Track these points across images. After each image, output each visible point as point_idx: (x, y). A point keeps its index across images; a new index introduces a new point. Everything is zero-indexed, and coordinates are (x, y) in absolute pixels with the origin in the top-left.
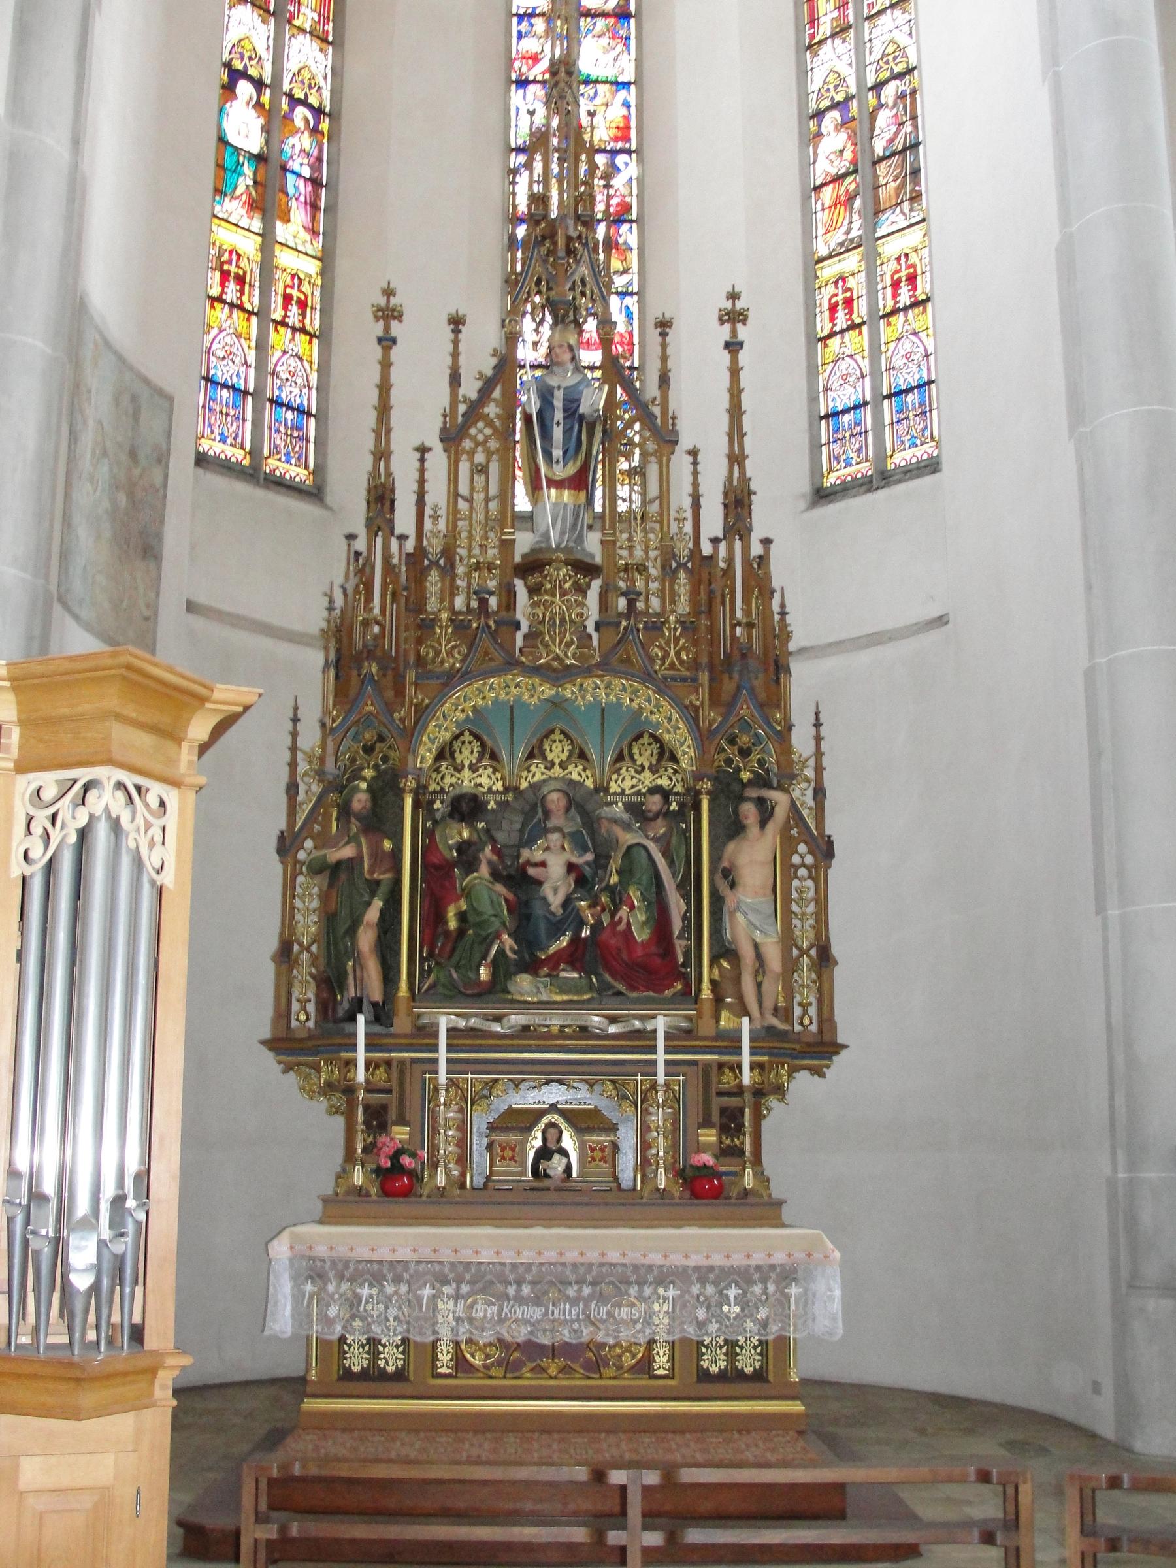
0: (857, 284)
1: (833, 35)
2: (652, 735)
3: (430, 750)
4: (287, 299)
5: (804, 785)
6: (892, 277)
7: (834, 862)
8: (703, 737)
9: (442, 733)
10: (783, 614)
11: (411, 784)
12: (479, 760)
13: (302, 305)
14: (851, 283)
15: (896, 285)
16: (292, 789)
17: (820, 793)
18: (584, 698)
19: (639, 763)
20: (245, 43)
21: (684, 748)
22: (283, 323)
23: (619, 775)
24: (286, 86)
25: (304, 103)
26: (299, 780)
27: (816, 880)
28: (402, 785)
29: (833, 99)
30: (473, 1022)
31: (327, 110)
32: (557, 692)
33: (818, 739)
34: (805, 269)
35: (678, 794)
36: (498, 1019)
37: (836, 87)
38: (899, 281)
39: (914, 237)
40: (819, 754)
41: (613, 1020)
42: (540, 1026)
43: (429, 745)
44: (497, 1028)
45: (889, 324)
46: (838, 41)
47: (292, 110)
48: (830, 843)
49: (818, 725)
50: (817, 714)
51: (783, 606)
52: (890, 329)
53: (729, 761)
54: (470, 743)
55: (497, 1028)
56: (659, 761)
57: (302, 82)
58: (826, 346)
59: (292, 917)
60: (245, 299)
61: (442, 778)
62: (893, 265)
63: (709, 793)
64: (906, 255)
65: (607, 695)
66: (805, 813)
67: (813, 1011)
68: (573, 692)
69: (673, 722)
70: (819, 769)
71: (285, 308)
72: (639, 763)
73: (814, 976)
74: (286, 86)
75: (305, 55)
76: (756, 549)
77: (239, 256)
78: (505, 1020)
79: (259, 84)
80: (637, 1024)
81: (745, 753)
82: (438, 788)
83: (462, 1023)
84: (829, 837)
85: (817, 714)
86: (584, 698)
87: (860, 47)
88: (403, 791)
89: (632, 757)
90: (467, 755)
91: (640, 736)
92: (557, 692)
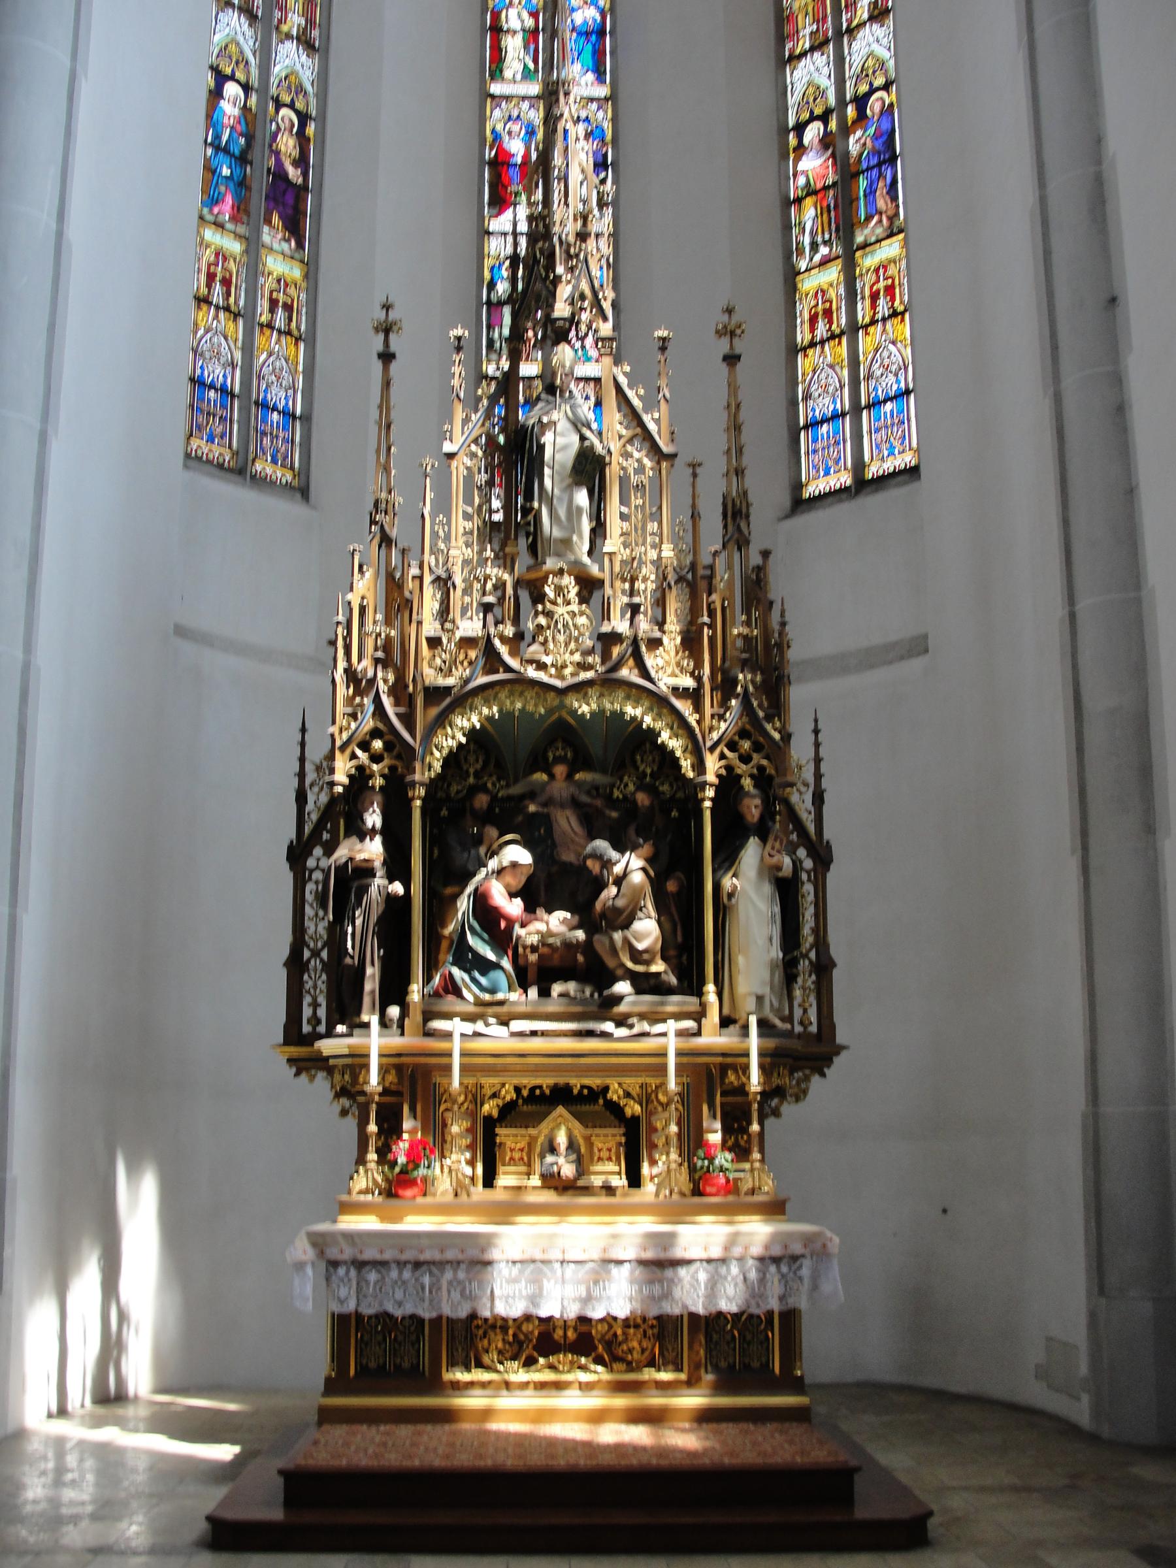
0: (837, 293)
1: (813, 49)
4: (273, 303)
6: (871, 288)
10: (783, 624)
13: (288, 308)
14: (832, 293)
15: (875, 297)
17: (819, 798)
20: (233, 48)
22: (270, 326)
24: (273, 91)
25: (291, 106)
29: (812, 112)
31: (314, 114)
33: (817, 745)
34: (786, 281)
37: (815, 99)
38: (878, 291)
39: (891, 249)
40: (818, 760)
45: (867, 334)
46: (817, 55)
47: (277, 112)
48: (828, 846)
49: (816, 732)
50: (816, 721)
51: (782, 615)
52: (869, 339)
56: (660, 767)
57: (289, 87)
58: (806, 356)
60: (232, 300)
62: (870, 278)
64: (885, 267)
66: (804, 816)
70: (818, 776)
71: (272, 310)
74: (273, 91)
75: (289, 58)
76: (755, 559)
77: (225, 259)
79: (246, 88)
85: (816, 721)
87: (840, 61)
89: (634, 763)
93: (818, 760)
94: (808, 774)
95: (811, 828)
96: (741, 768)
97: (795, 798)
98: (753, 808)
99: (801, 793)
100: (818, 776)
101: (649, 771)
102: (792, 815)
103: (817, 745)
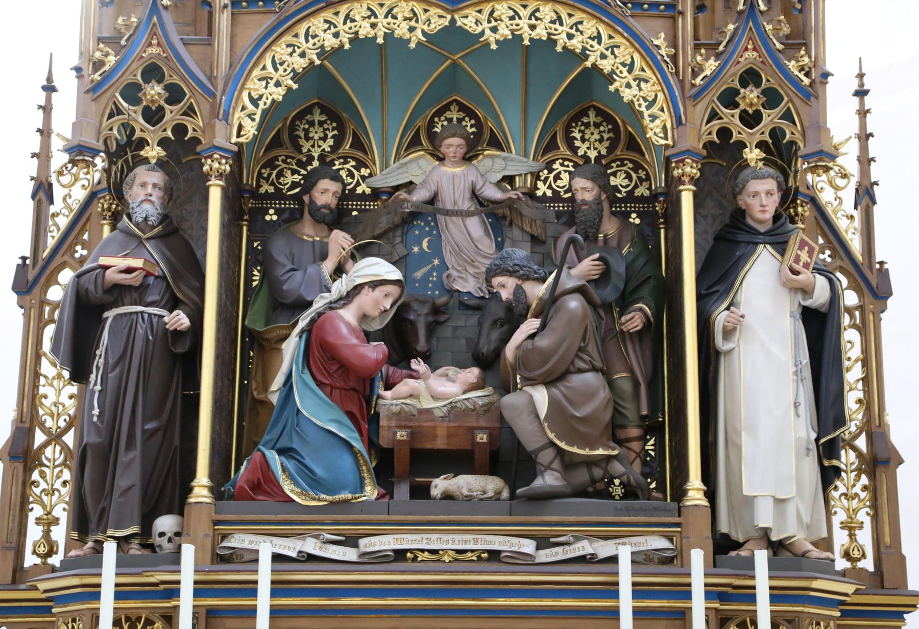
2: (599, 112)
3: (251, 116)
5: (840, 182)
7: (890, 302)
8: (681, 91)
9: (272, 88)
11: (217, 165)
12: (334, 148)
16: (43, 191)
17: (866, 195)
18: (494, 30)
19: (581, 153)
21: (655, 110)
23: (551, 171)
26: (53, 179)
27: (862, 329)
28: (206, 168)
30: (311, 546)
32: (453, 21)
33: (863, 113)
35: (642, 199)
36: (351, 541)
40: (864, 137)
41: (543, 543)
42: (423, 551)
43: (250, 107)
44: (350, 554)
48: (884, 274)
50: (861, 76)
53: (724, 133)
54: (321, 123)
55: (350, 554)
56: (611, 150)
59: (35, 386)
61: (280, 174)
63: (693, 180)
65: (533, 27)
66: (842, 224)
67: (865, 537)
68: (477, 22)
69: (637, 72)
70: (865, 161)
72: (581, 153)
73: (864, 480)
78: (362, 542)
80: (584, 548)
81: (751, 120)
82: (271, 190)
83: (290, 547)
84: (881, 263)
85: (861, 76)
86: (494, 30)
88: (206, 177)
90: (318, 143)
91: (584, 112)
92: (453, 21)
93: (864, 137)
94: (849, 160)
95: (855, 244)
96: (739, 132)
97: (826, 196)
98: (761, 197)
99: (837, 188)
100: (865, 161)
101: (593, 154)
102: (824, 222)
103: (863, 113)
